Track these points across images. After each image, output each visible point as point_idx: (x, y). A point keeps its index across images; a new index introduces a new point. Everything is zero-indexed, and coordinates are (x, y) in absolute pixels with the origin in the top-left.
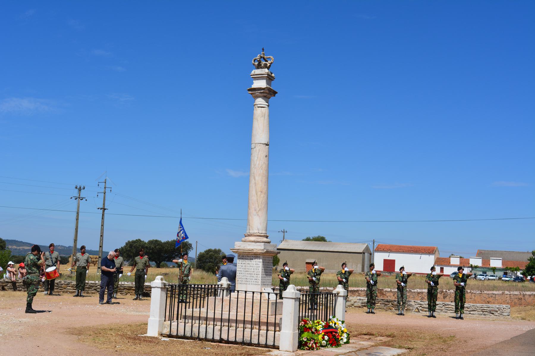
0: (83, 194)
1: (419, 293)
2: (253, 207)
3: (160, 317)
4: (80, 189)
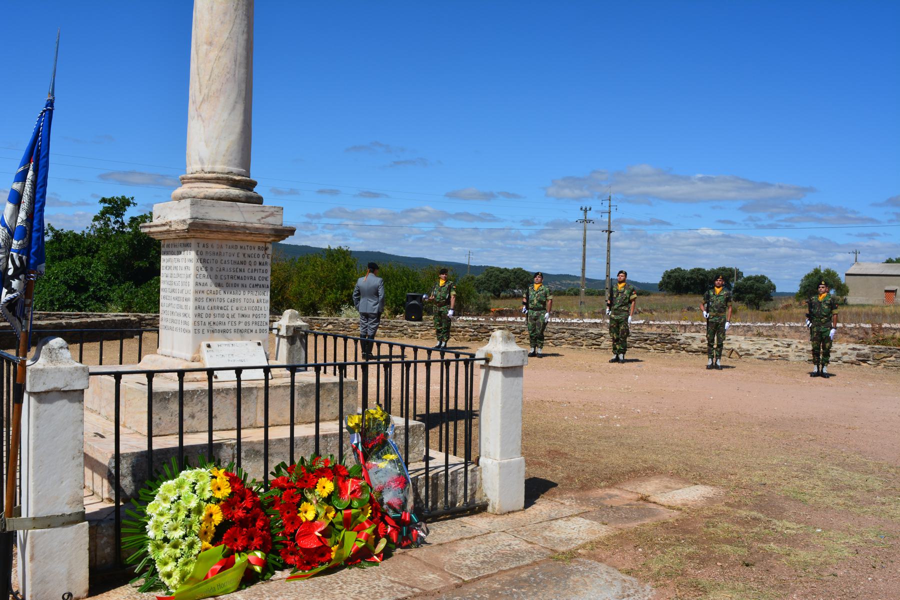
0: (590, 215)
4: (586, 211)
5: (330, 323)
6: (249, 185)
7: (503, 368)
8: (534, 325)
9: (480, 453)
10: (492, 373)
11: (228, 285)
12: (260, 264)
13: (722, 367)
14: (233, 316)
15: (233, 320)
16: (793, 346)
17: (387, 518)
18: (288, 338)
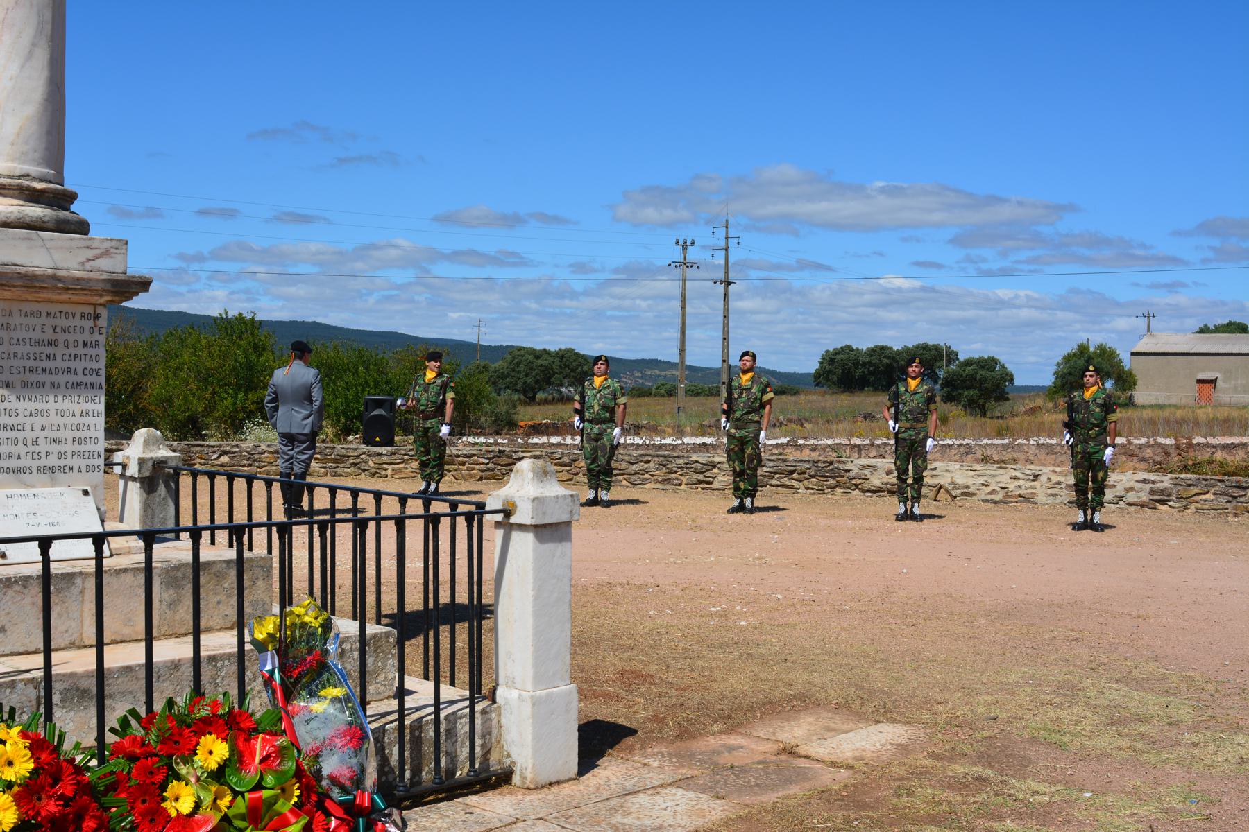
0: (692, 254)
4: (685, 246)
5: (225, 453)
6: (63, 199)
7: (536, 526)
8: (595, 450)
9: (496, 681)
10: (516, 536)
11: (24, 385)
12: (85, 344)
13: (922, 517)
14: (35, 442)
15: (36, 449)
16: (1043, 479)
17: (328, 804)
18: (142, 480)
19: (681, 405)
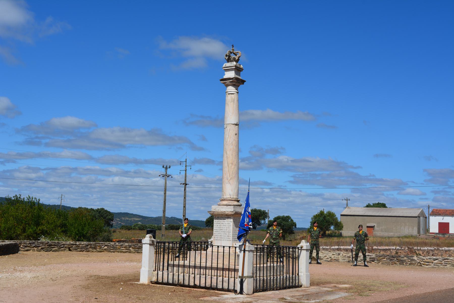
0: (169, 172)
1: (446, 251)
2: (225, 176)
3: (149, 268)
5: (106, 246)
16: (341, 255)
19: (163, 234)
